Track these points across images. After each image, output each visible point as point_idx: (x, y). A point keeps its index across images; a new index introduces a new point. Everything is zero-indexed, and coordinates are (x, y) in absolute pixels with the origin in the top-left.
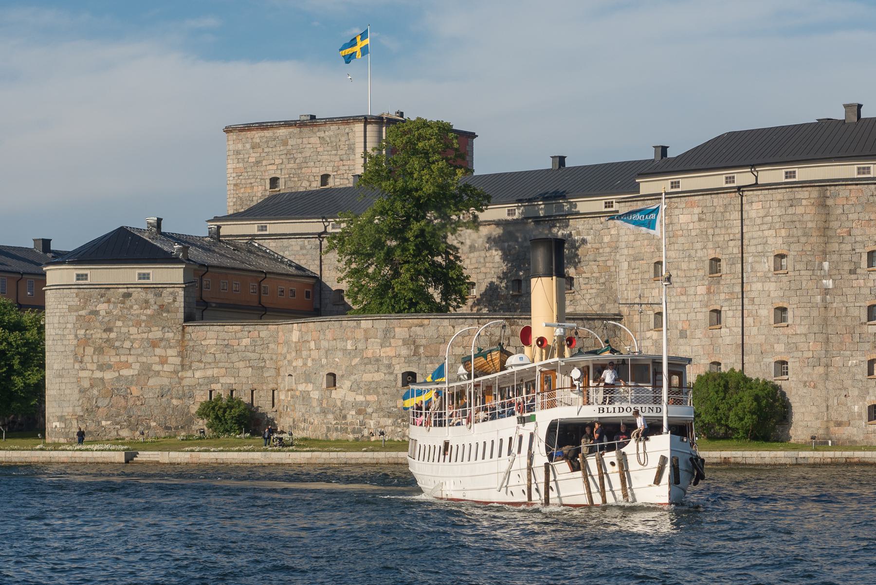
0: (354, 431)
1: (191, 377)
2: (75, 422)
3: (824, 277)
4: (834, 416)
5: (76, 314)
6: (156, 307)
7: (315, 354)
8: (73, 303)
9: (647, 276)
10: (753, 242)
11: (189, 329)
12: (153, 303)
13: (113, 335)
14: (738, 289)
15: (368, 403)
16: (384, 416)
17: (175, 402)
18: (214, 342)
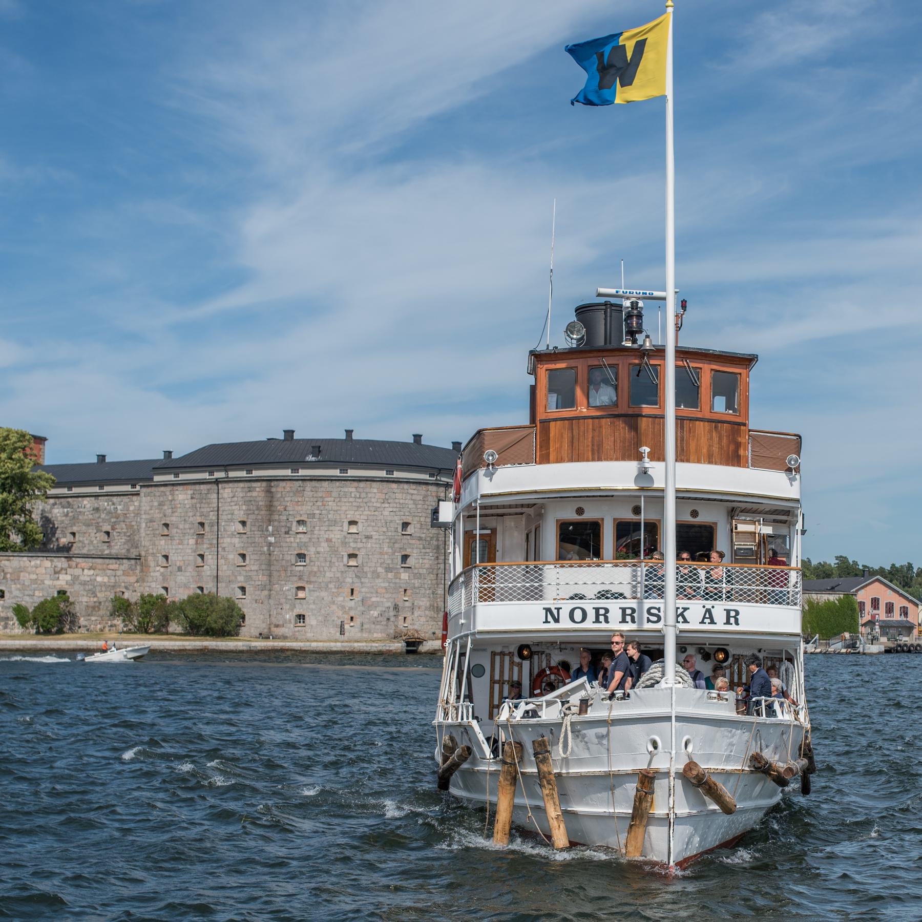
3: (269, 535)
4: (274, 621)
9: (157, 532)
10: (225, 513)
14: (215, 542)
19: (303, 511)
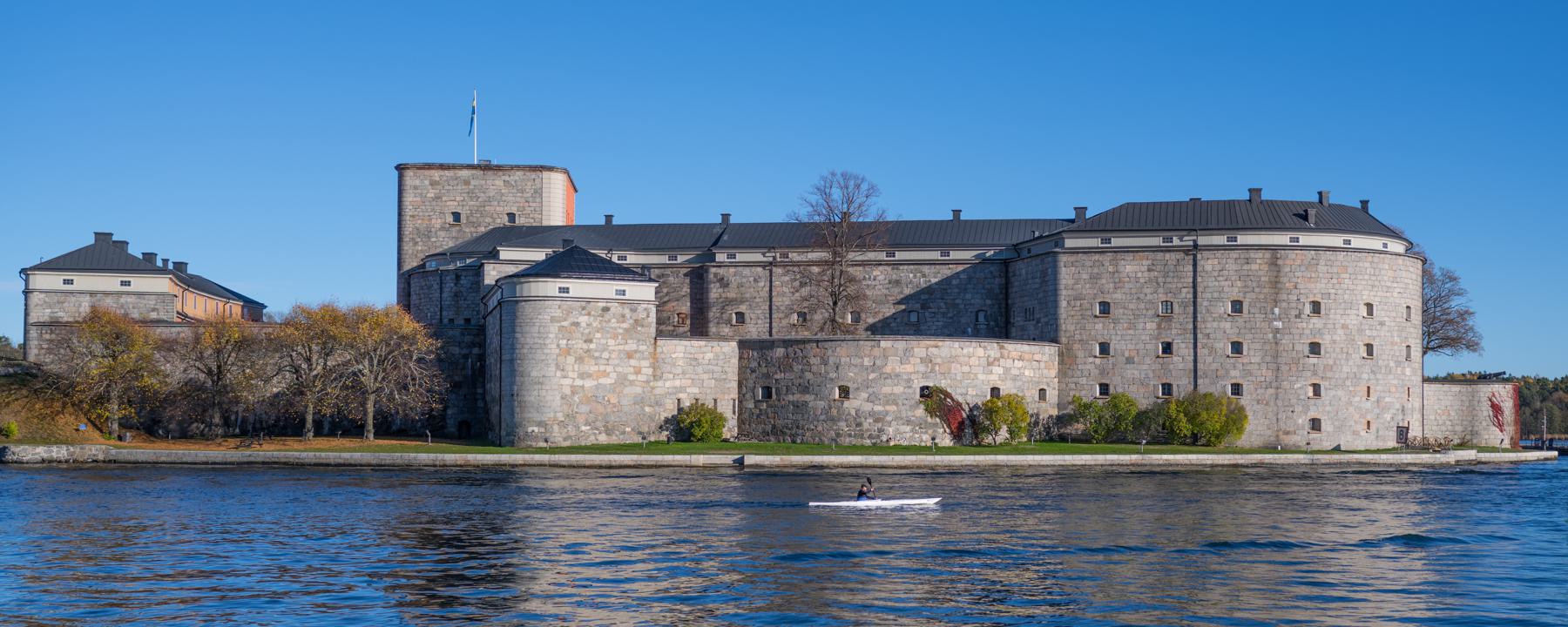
0: (870, 437)
1: (662, 387)
13: (592, 346)
15: (887, 413)
17: (647, 409)
19: (1316, 289)
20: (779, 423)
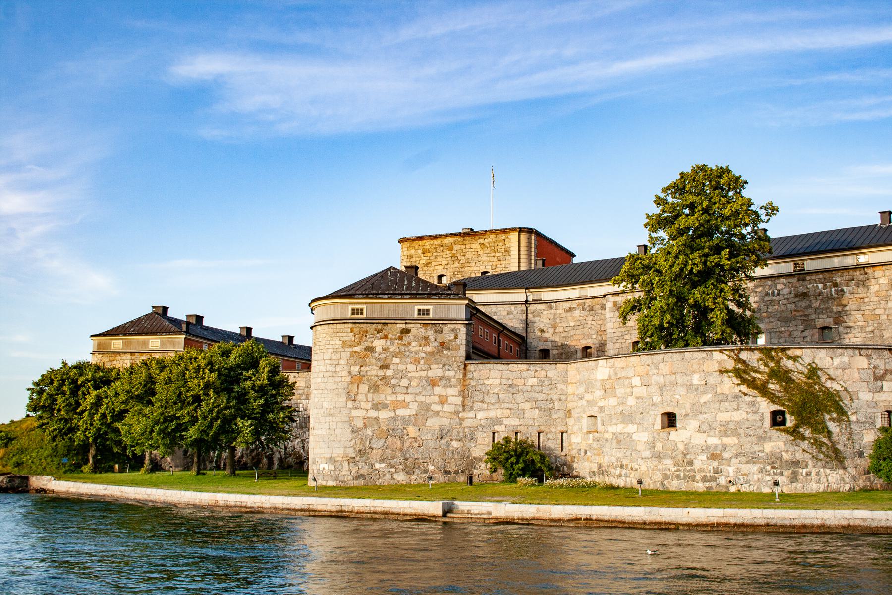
0: (704, 480)
2: (346, 464)
5: (350, 349)
6: (436, 344)
7: (641, 391)
8: (347, 339)
11: (471, 368)
12: (433, 339)
13: (389, 373)
15: (724, 447)
16: (747, 462)
17: (455, 444)
18: (498, 381)
20: (605, 461)
